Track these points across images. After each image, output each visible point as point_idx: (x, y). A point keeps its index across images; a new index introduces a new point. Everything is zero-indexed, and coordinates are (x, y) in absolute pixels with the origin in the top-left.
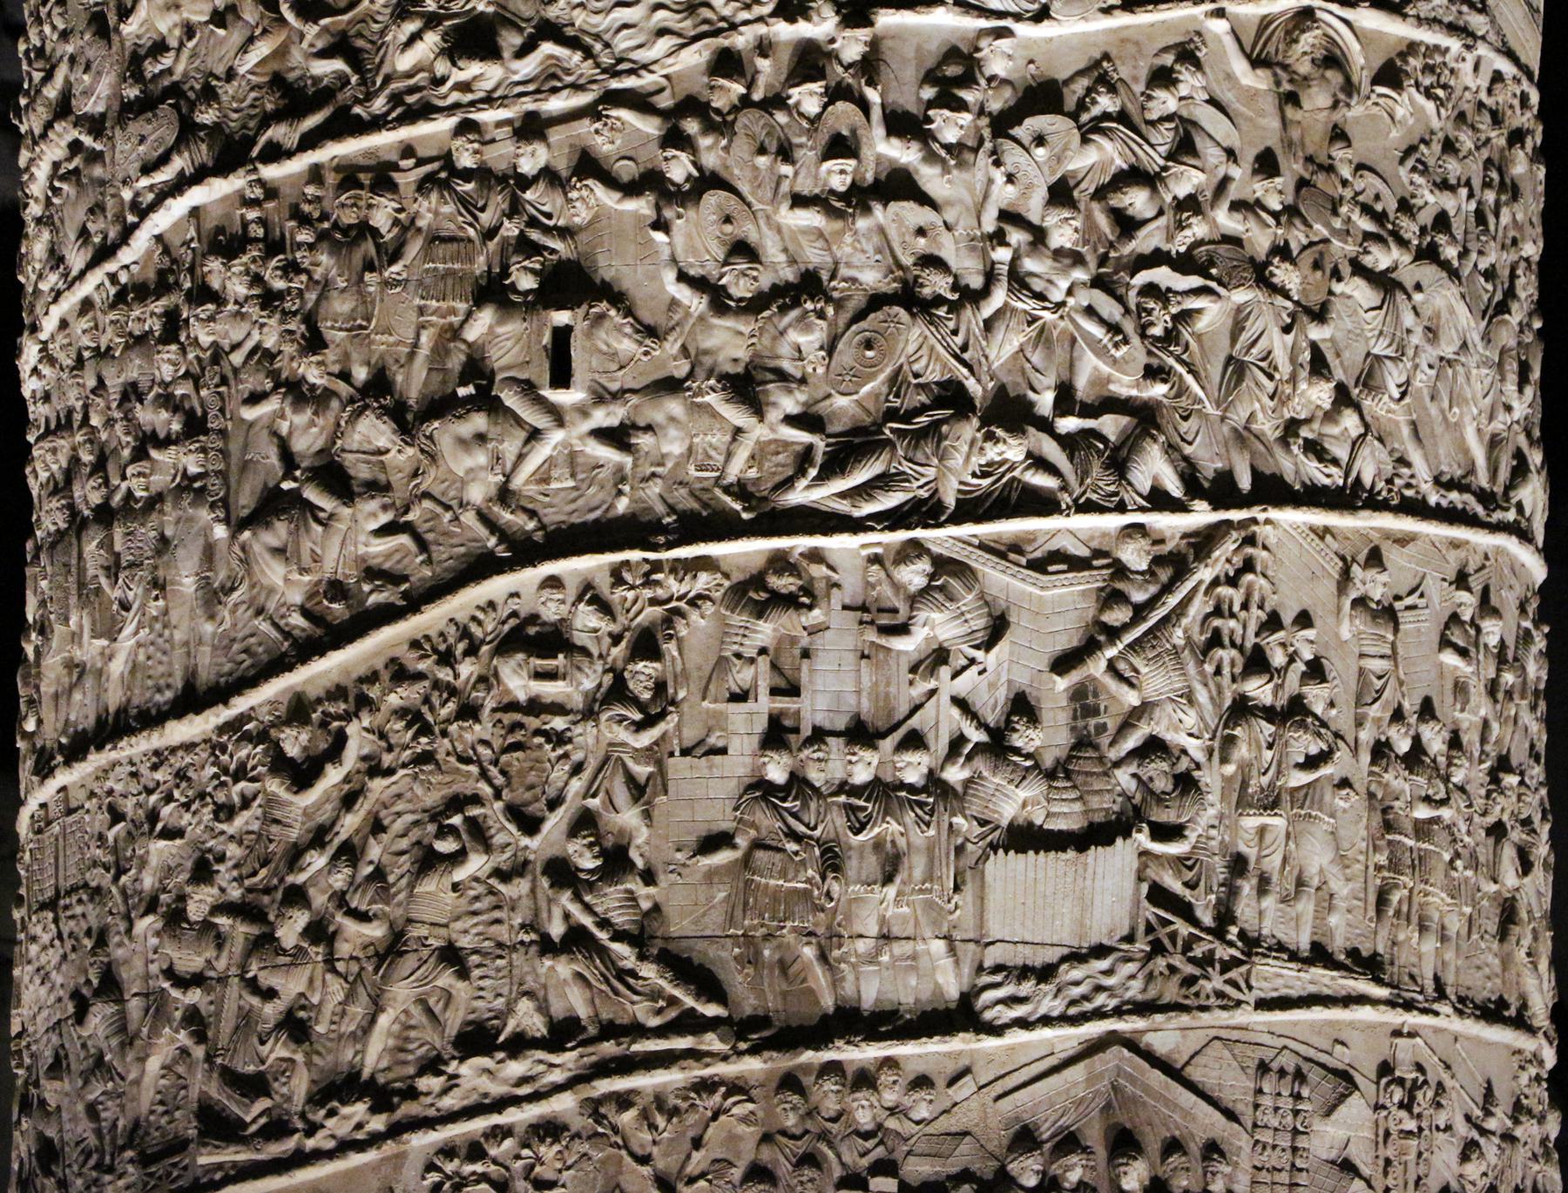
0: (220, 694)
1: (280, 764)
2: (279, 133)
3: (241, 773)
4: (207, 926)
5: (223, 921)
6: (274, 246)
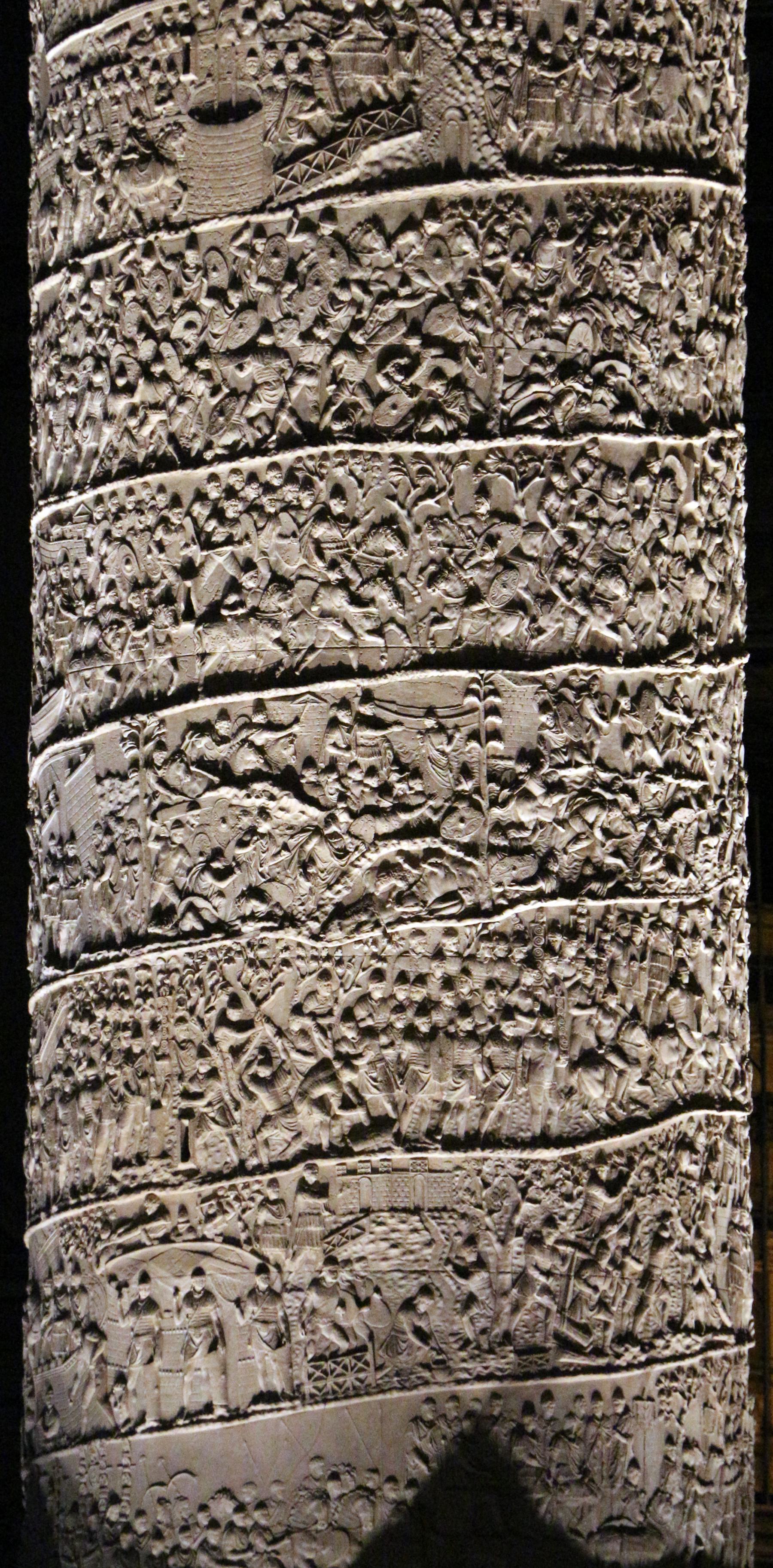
0: (559, 1142)
1: (594, 1179)
2: (595, 886)
3: (577, 1182)
4: (554, 1250)
5: (561, 1248)
6: (590, 939)
